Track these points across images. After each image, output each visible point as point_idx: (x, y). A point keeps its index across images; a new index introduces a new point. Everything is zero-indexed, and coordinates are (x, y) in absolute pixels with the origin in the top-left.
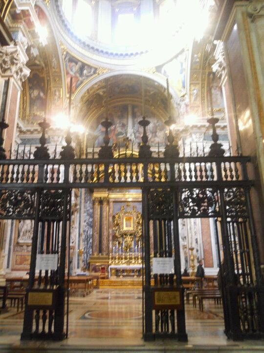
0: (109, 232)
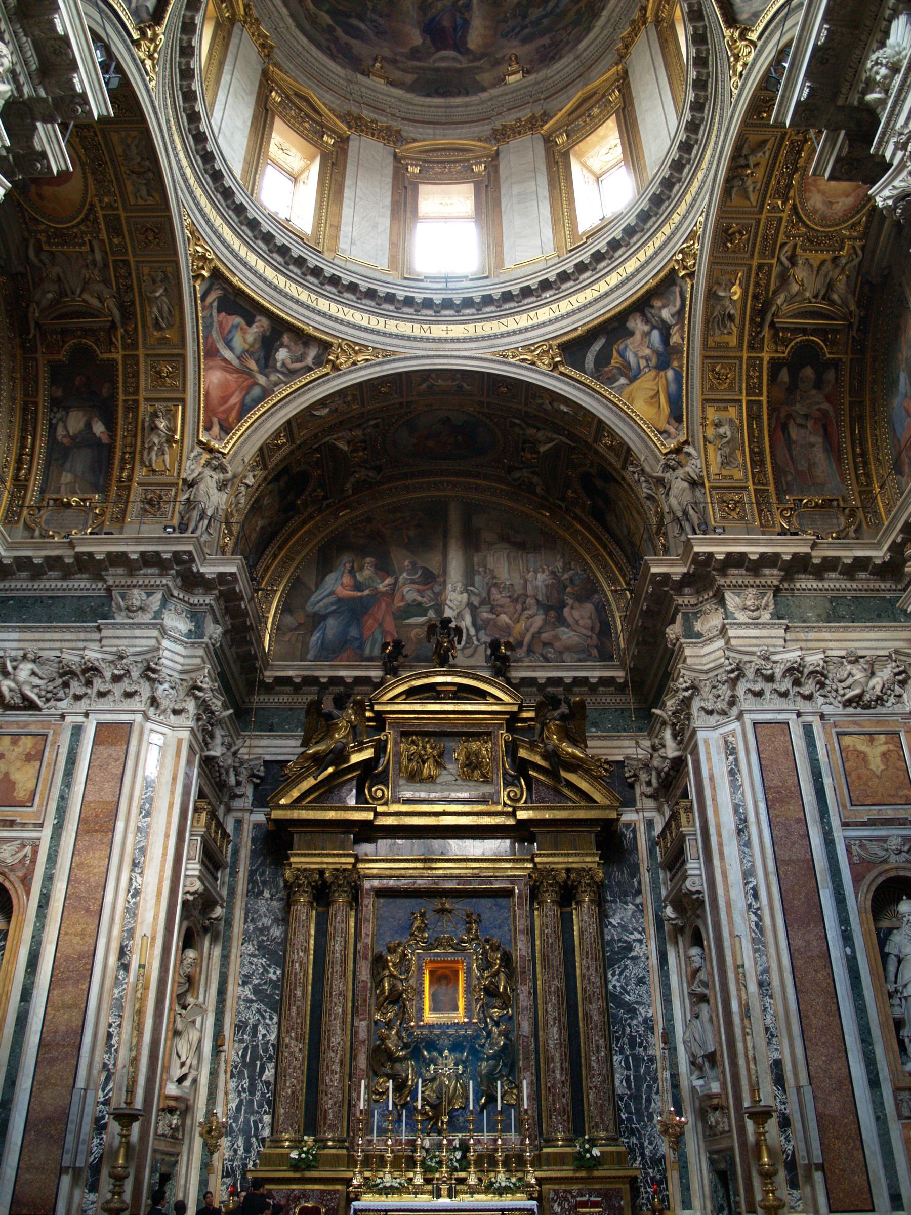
0: (354, 1033)
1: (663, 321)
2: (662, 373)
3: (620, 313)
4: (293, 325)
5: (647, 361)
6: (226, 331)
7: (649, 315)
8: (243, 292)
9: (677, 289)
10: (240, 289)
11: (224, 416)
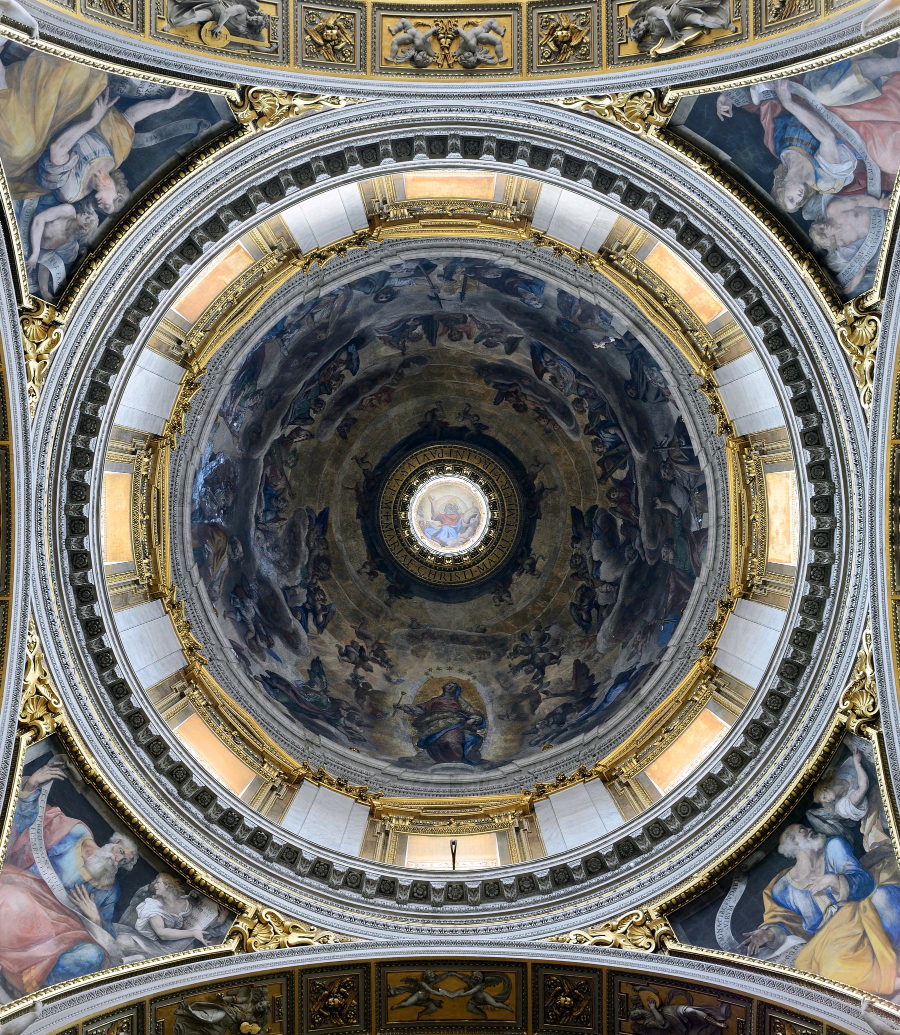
1: (843, 821)
2: (864, 903)
3: (763, 832)
4: (178, 863)
5: (830, 896)
6: (56, 838)
7: (816, 822)
8: (100, 785)
9: (855, 760)
10: (94, 778)
11: (16, 969)
